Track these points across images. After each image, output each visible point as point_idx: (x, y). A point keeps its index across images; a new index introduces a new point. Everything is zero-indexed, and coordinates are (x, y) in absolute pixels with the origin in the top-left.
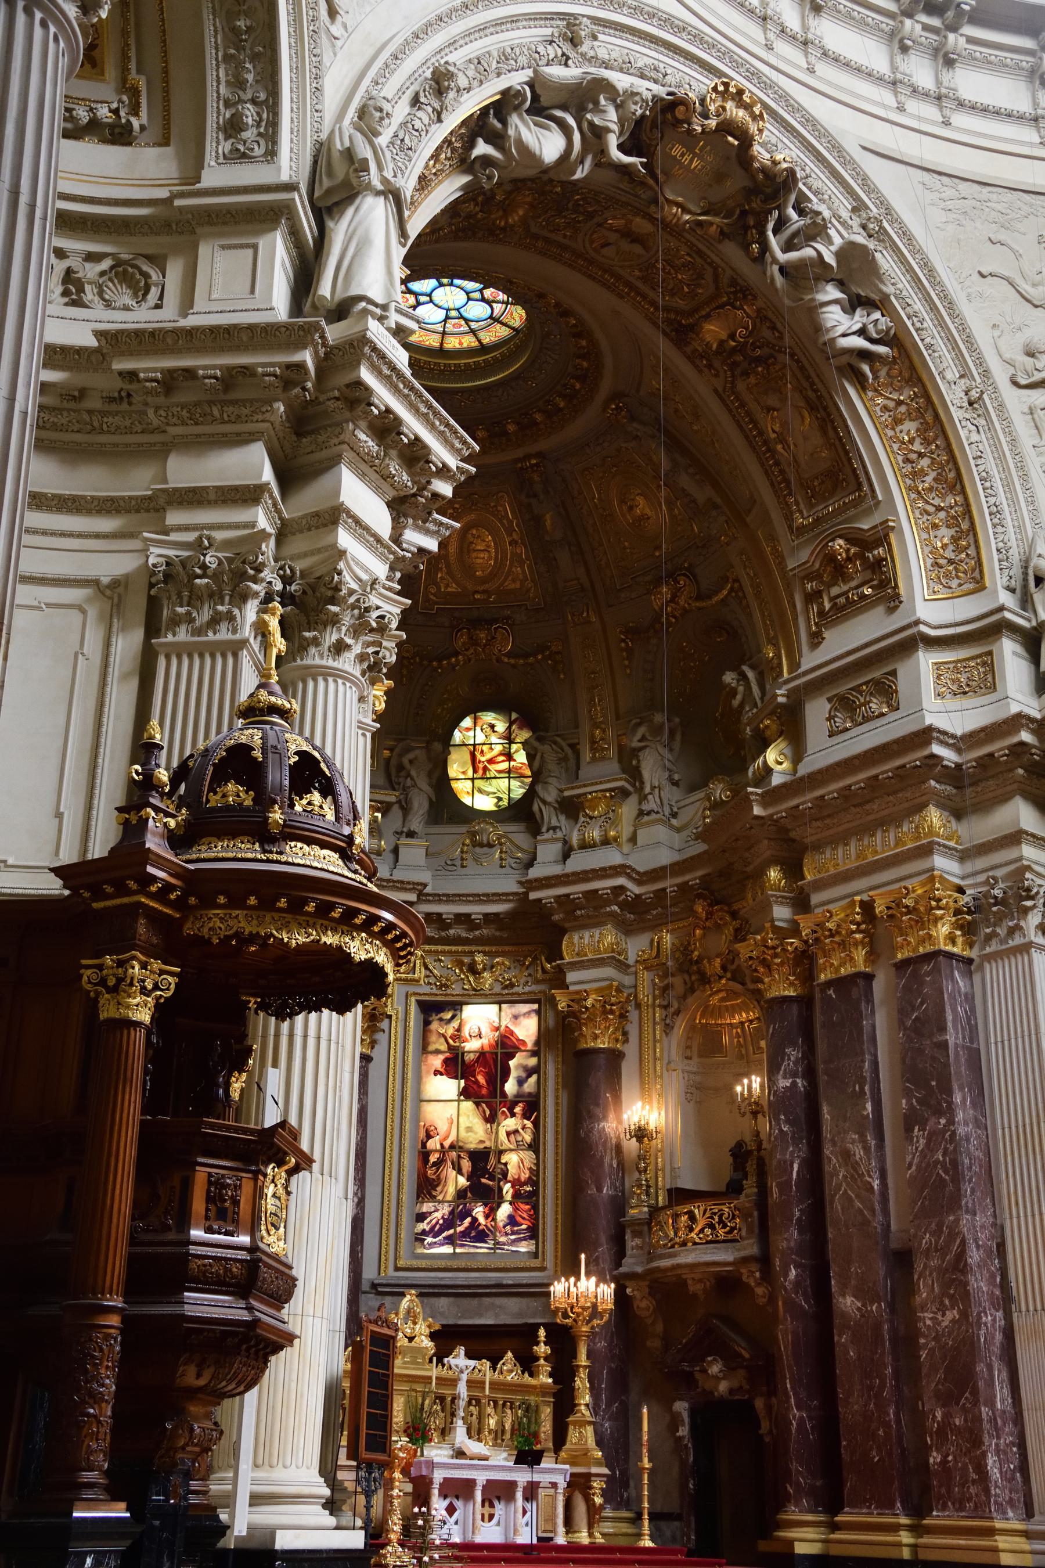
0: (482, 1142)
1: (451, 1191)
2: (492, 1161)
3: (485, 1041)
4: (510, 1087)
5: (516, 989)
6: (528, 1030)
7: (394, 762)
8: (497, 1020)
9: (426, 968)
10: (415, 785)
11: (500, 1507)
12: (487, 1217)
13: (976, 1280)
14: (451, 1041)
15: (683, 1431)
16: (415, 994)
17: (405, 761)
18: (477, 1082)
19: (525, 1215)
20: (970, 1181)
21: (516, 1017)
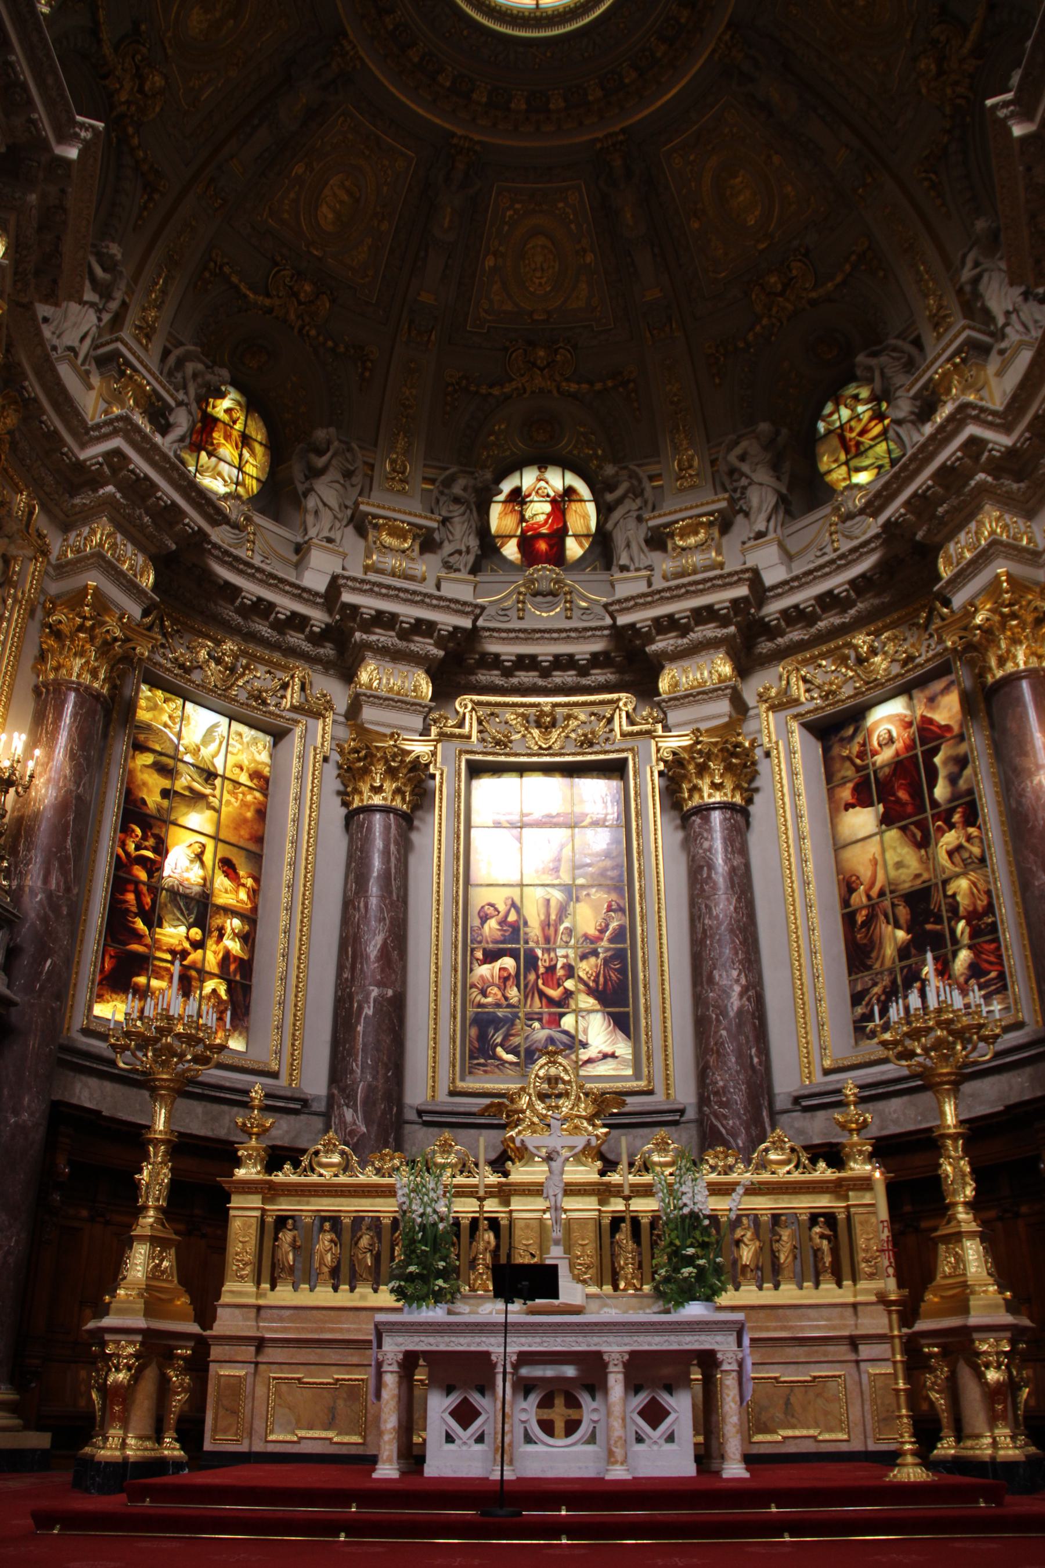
0: (917, 876)
2: (937, 897)
3: (899, 745)
4: (941, 791)
5: (918, 661)
6: (950, 710)
8: (908, 712)
9: (805, 680)
11: (594, 1405)
14: (858, 761)
16: (795, 717)
18: (898, 800)
19: (992, 959)
21: (932, 700)
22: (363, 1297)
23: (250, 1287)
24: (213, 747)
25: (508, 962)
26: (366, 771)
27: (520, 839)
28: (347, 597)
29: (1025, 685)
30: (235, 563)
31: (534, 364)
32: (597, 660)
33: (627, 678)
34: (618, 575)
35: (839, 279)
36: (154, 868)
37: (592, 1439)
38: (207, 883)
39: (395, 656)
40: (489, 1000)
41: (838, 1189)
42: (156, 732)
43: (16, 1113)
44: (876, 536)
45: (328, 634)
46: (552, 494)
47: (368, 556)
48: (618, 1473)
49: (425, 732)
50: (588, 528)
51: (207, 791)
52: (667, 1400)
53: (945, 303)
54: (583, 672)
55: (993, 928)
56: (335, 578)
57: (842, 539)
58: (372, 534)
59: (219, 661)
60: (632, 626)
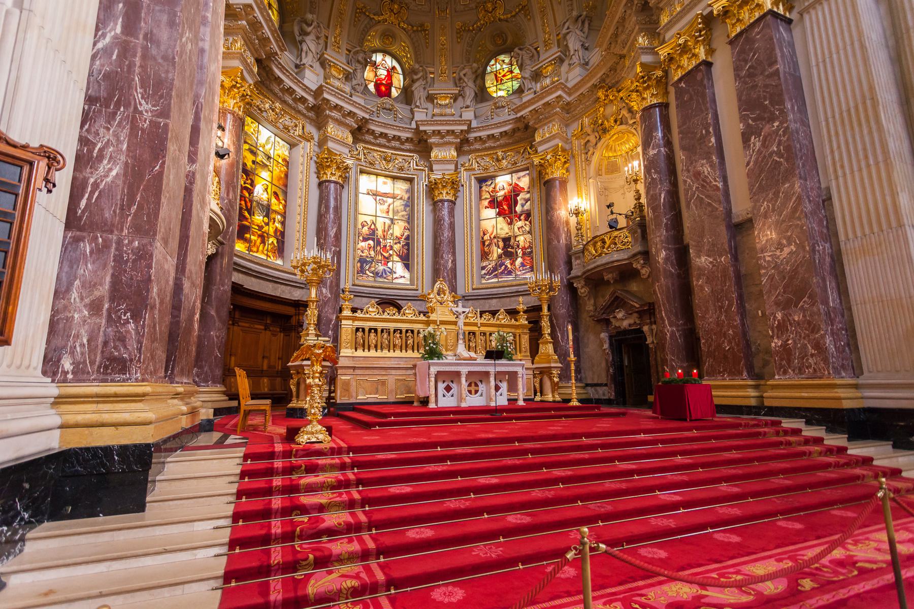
1: (495, 256)
2: (512, 240)
3: (506, 191)
4: (518, 209)
7: (457, 77)
9: (478, 163)
12: (511, 264)
13: (810, 222)
15: (606, 346)
17: (462, 74)
20: (801, 158)
21: (519, 178)
22: (385, 353)
25: (371, 242)
26: (329, 166)
27: (376, 200)
29: (557, 182)
31: (392, 11)
35: (513, 13)
36: (251, 192)
37: (481, 395)
38: (269, 200)
40: (364, 254)
41: (516, 327)
42: (249, 136)
43: (223, 286)
44: (513, 119)
51: (268, 164)
52: (500, 384)
53: (551, 38)
54: (402, 143)
55: (532, 252)
56: (321, 86)
57: (495, 116)
59: (273, 110)
60: (425, 131)
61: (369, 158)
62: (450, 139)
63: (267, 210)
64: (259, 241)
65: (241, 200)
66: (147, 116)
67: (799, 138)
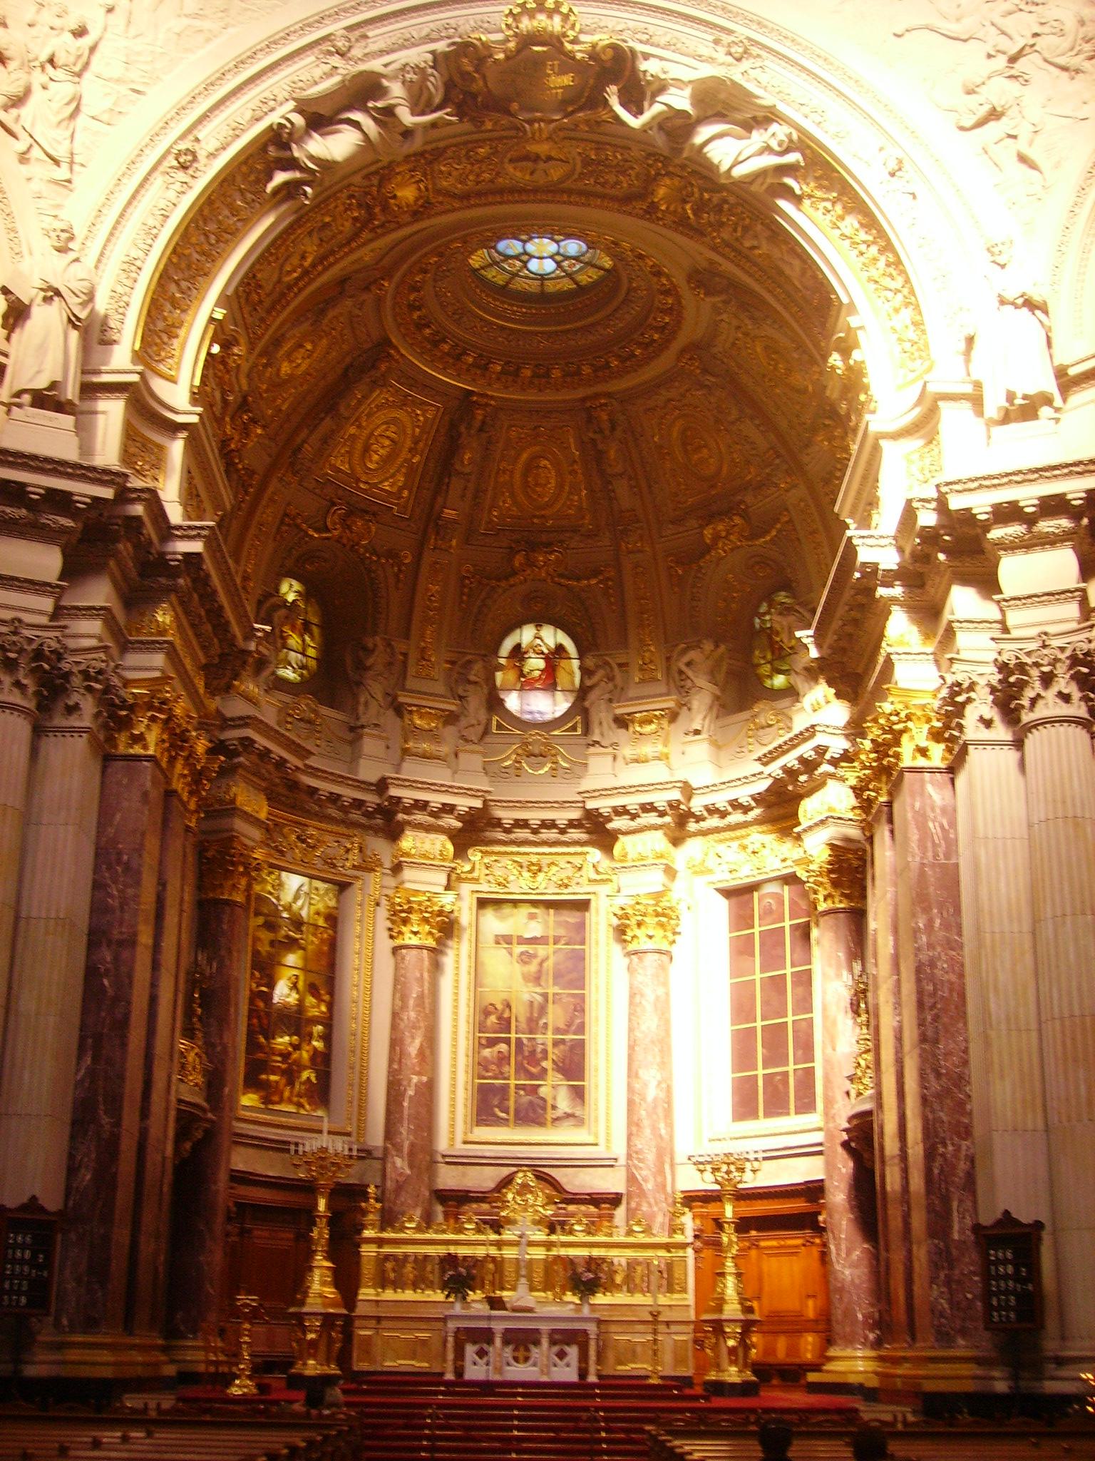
10: (694, 686)
23: (372, 1291)
24: (300, 903)
25: (503, 1047)
26: (405, 922)
27: (511, 954)
28: (394, 792)
30: (314, 772)
32: (572, 824)
33: (594, 837)
34: (592, 750)
36: (268, 997)
37: (534, 1365)
38: (301, 1001)
39: (428, 829)
45: (379, 809)
46: (546, 651)
47: (406, 741)
48: (545, 1379)
49: (448, 888)
50: (573, 683)
51: (298, 936)
58: (407, 716)
59: (303, 841)
61: (498, 872)
62: (652, 818)
63: (294, 1020)
64: (283, 1081)
65: (250, 1018)
66: (107, 1127)
67: (933, 974)
